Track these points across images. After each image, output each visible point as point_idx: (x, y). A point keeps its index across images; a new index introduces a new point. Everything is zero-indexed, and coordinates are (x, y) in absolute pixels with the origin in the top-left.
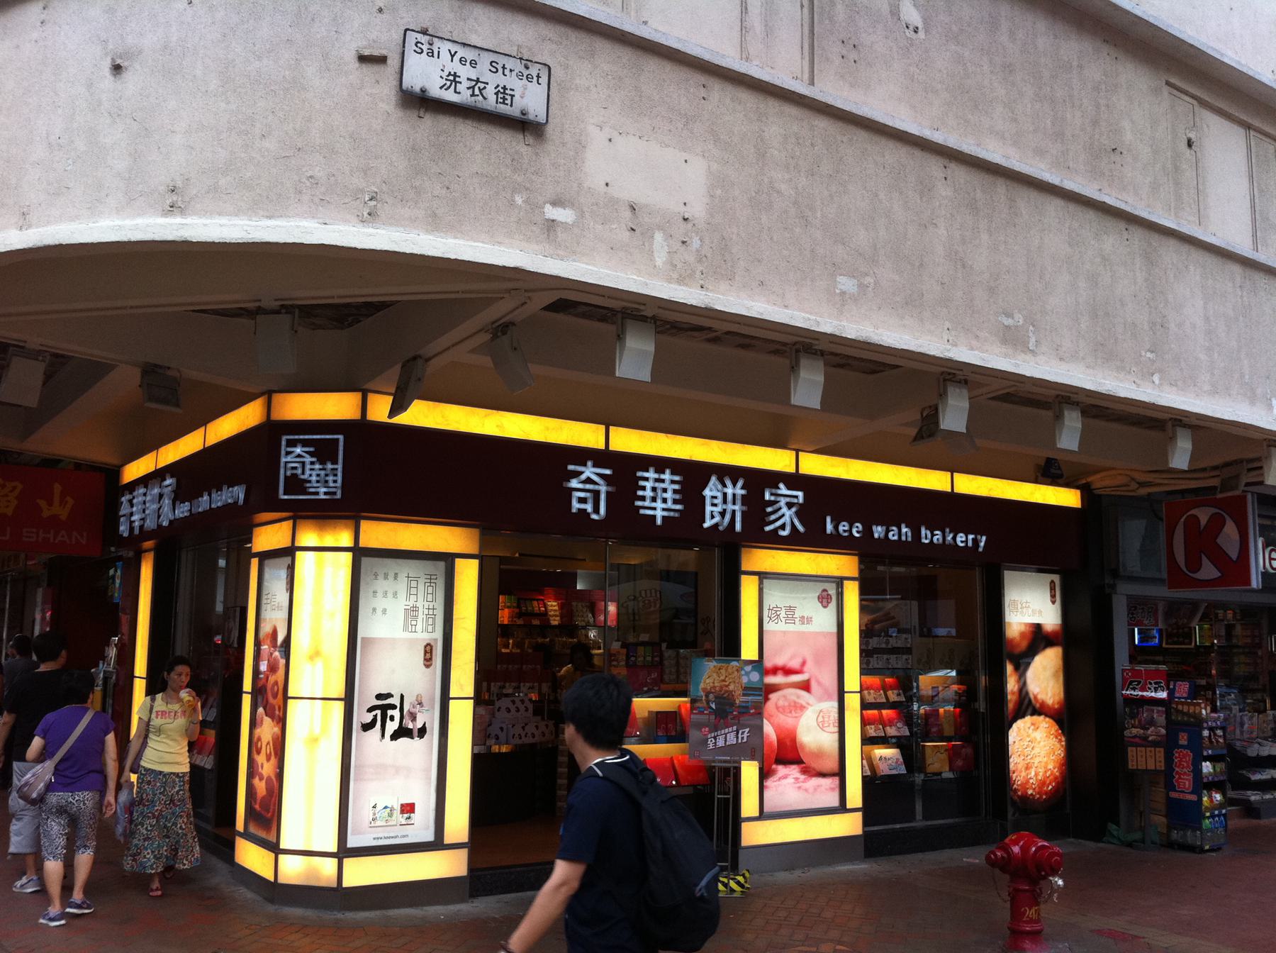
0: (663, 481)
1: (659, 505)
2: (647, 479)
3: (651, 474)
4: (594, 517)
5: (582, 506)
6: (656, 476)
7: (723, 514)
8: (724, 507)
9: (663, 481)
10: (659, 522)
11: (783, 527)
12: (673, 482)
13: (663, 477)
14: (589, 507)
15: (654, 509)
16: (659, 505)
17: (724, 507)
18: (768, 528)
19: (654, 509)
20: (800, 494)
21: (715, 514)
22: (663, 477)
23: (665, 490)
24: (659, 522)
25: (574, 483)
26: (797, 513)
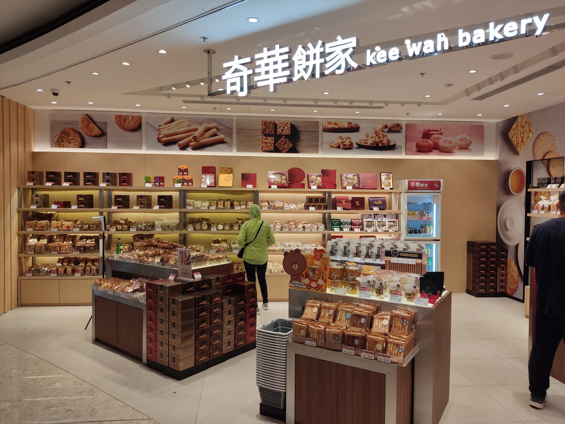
1: (272, 75)
2: (262, 59)
5: (233, 88)
6: (271, 53)
9: (274, 56)
25: (227, 76)
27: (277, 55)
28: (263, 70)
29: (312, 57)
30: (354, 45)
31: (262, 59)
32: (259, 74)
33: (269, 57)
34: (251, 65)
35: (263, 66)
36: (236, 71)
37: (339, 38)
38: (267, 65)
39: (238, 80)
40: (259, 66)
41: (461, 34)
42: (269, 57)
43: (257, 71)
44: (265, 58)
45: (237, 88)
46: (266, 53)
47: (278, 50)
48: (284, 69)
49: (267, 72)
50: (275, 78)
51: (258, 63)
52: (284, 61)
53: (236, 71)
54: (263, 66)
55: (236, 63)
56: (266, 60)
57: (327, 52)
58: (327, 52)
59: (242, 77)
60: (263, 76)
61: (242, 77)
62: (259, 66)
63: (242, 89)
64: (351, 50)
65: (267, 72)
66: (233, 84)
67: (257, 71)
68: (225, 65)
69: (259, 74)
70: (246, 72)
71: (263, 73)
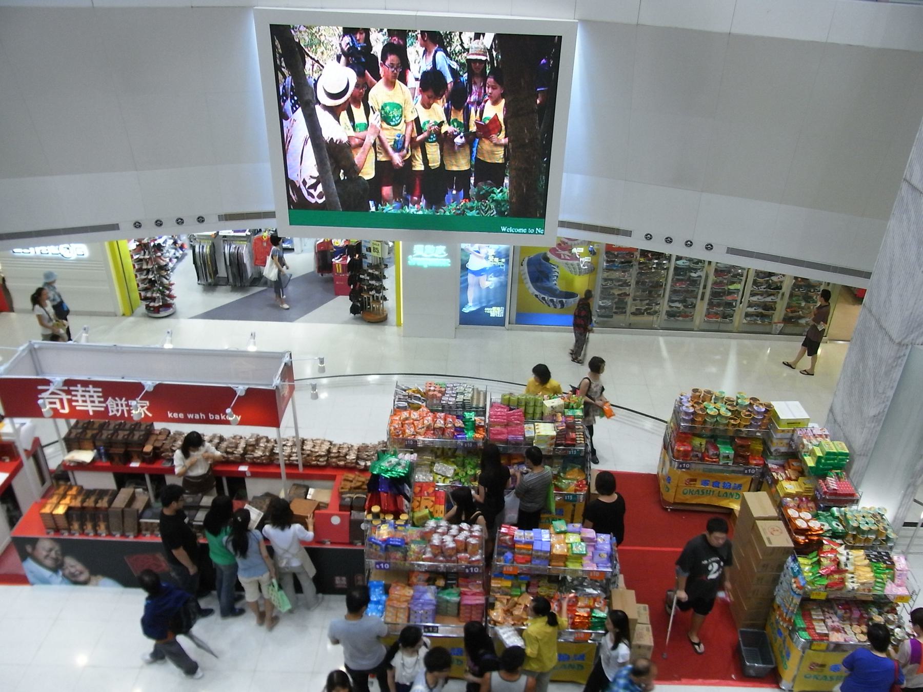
0: (89, 392)
3: (79, 387)
6: (84, 389)
7: (118, 411)
10: (91, 413)
12: (95, 392)
13: (87, 389)
14: (58, 406)
15: (87, 406)
16: (89, 404)
19: (87, 406)
22: (87, 389)
23: (92, 396)
24: (91, 413)
25: (44, 395)
26: (147, 409)
29: (119, 405)
31: (77, 391)
32: (77, 401)
33: (83, 391)
39: (57, 401)
40: (76, 396)
41: (192, 417)
42: (83, 391)
43: (74, 398)
45: (58, 406)
59: (61, 400)
66: (55, 403)
67: (74, 398)
69: (77, 401)
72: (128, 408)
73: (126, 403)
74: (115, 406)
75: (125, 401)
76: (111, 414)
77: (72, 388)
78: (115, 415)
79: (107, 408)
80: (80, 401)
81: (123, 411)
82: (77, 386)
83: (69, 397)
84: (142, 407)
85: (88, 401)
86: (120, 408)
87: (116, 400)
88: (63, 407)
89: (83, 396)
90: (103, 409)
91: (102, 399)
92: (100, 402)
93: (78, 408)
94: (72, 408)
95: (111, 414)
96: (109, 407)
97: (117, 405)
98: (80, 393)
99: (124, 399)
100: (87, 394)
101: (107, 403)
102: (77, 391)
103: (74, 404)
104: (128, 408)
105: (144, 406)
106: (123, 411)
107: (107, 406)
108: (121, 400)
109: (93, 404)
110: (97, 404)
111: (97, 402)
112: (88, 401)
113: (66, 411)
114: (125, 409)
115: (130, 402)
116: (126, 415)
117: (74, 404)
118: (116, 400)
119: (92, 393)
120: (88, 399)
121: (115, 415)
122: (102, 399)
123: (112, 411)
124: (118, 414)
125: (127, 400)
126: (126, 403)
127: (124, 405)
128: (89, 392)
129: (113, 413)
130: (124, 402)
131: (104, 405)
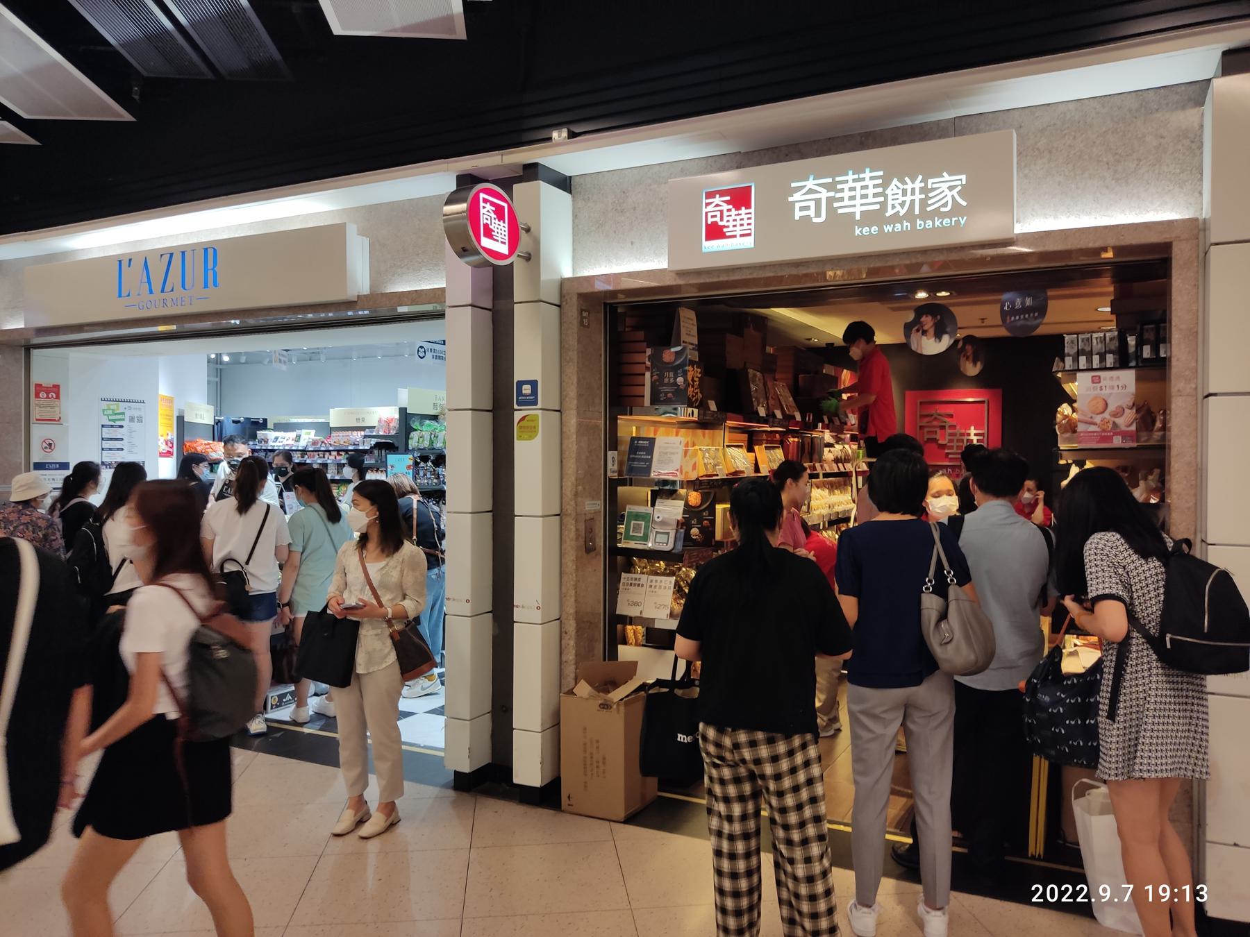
0: (863, 179)
4: (815, 220)
6: (856, 176)
7: (902, 204)
8: (904, 199)
10: (858, 217)
11: (945, 205)
12: (871, 178)
13: (861, 176)
15: (854, 206)
16: (858, 201)
17: (904, 199)
18: (929, 209)
19: (854, 206)
20: (963, 177)
21: (897, 205)
22: (861, 176)
24: (858, 217)
25: (797, 196)
27: (867, 179)
28: (846, 194)
30: (964, 182)
31: (846, 182)
32: (842, 199)
33: (854, 181)
34: (829, 187)
35: (846, 190)
36: (811, 191)
37: (945, 174)
38: (851, 189)
40: (842, 190)
42: (854, 181)
44: (850, 181)
45: (812, 213)
46: (851, 176)
47: (868, 174)
48: (875, 195)
49: (852, 198)
50: (862, 205)
51: (839, 187)
52: (875, 186)
53: (811, 191)
54: (846, 190)
55: (810, 183)
56: (851, 184)
57: (929, 187)
58: (929, 187)
60: (846, 202)
61: (818, 201)
62: (842, 190)
63: (818, 214)
64: (960, 188)
65: (852, 198)
67: (838, 195)
68: (793, 185)
69: (842, 199)
70: (824, 194)
71: (846, 199)
72: (923, 196)
73: (923, 185)
74: (900, 196)
75: (921, 182)
76: (890, 212)
77: (838, 179)
78: (898, 212)
79: (884, 205)
80: (846, 199)
81: (913, 202)
82: (847, 175)
83: (832, 194)
84: (951, 188)
85: (858, 197)
86: (909, 198)
87: (904, 183)
88: (818, 214)
89: (851, 189)
90: (877, 207)
91: (880, 190)
92: (875, 195)
93: (840, 211)
94: (831, 210)
95: (890, 212)
96: (890, 197)
97: (904, 193)
98: (846, 187)
99: (920, 177)
100: (858, 185)
101: (888, 192)
102: (846, 182)
103: (836, 205)
104: (923, 196)
105: (956, 186)
106: (913, 202)
107: (886, 196)
108: (913, 183)
109: (864, 201)
110: (871, 199)
111: (870, 196)
112: (858, 197)
113: (822, 219)
114: (918, 197)
115: (930, 181)
116: (917, 212)
117: (836, 205)
118: (904, 183)
119: (868, 182)
120: (858, 193)
121: (898, 212)
122: (880, 190)
123: (893, 207)
124: (902, 212)
125: (924, 180)
126: (923, 185)
127: (917, 191)
128: (863, 179)
129: (895, 211)
130: (918, 184)
131: (882, 199)
